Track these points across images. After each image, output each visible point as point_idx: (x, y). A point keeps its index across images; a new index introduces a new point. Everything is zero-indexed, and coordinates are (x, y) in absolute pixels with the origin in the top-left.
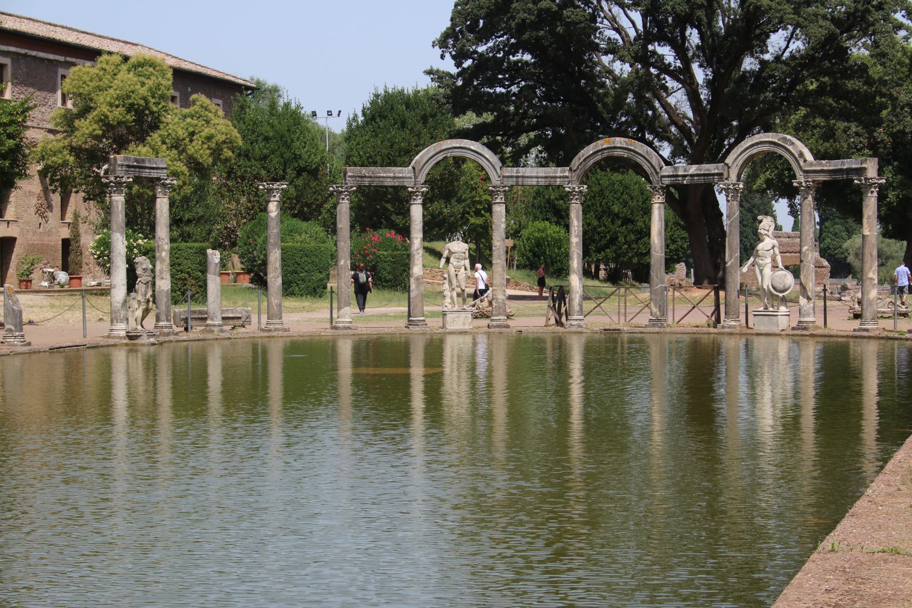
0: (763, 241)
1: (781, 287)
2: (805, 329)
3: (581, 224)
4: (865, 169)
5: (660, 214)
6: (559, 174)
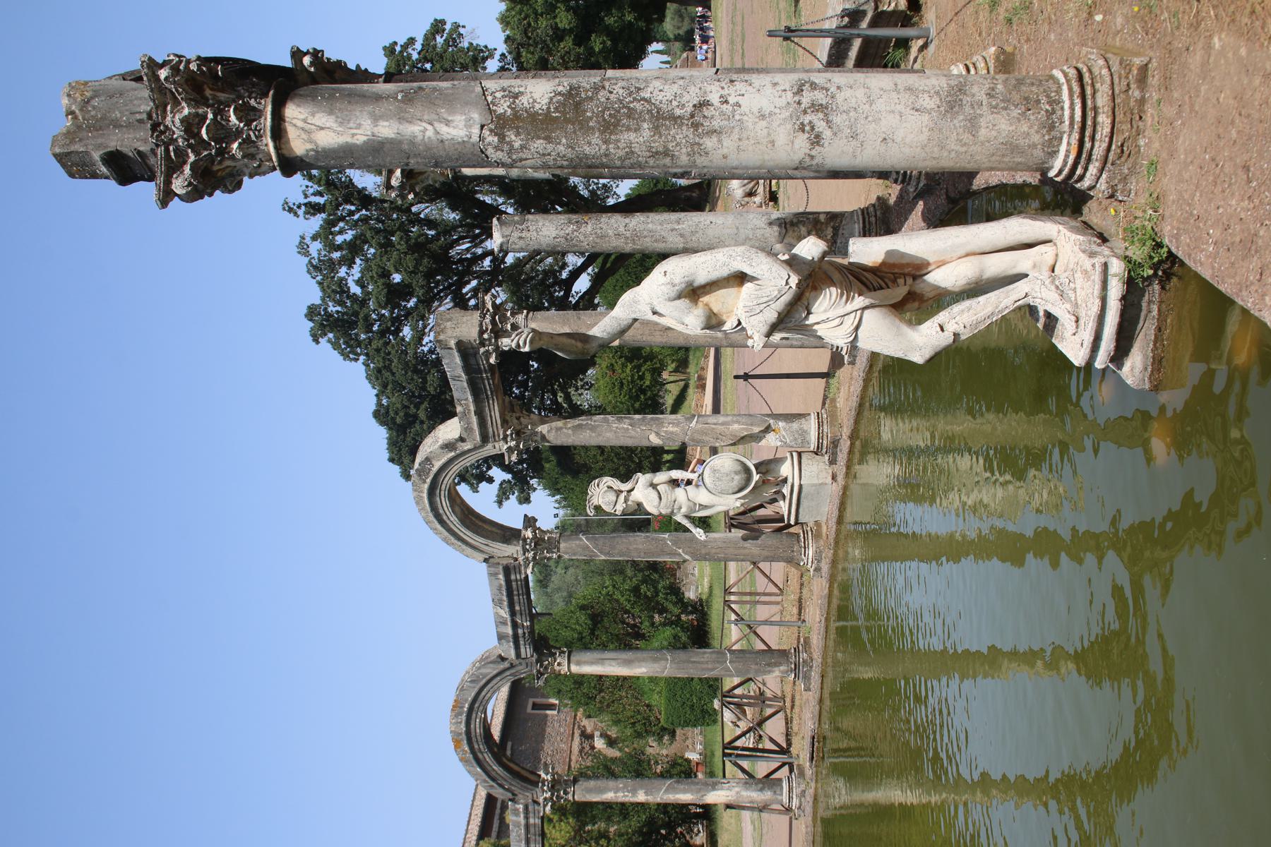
0: (639, 505)
1: (738, 479)
2: (835, 443)
3: (611, 783)
4: (460, 344)
5: (592, 663)
6: (522, 819)
